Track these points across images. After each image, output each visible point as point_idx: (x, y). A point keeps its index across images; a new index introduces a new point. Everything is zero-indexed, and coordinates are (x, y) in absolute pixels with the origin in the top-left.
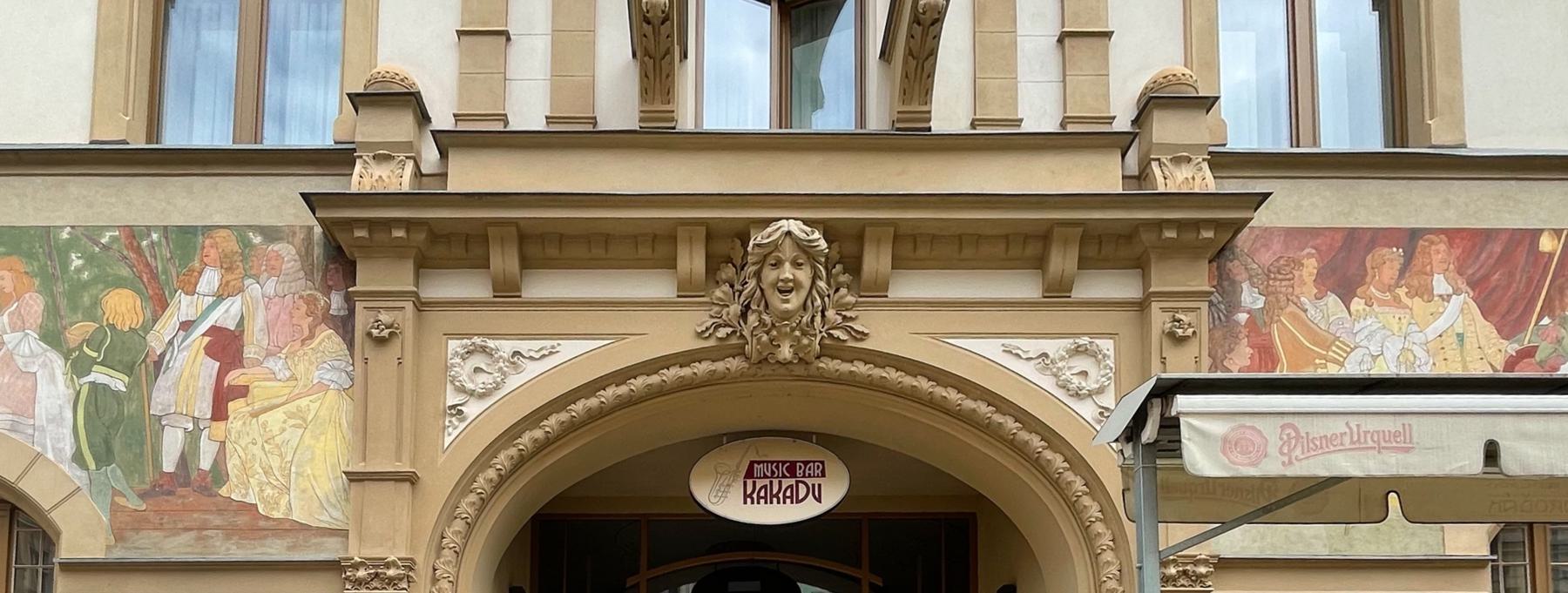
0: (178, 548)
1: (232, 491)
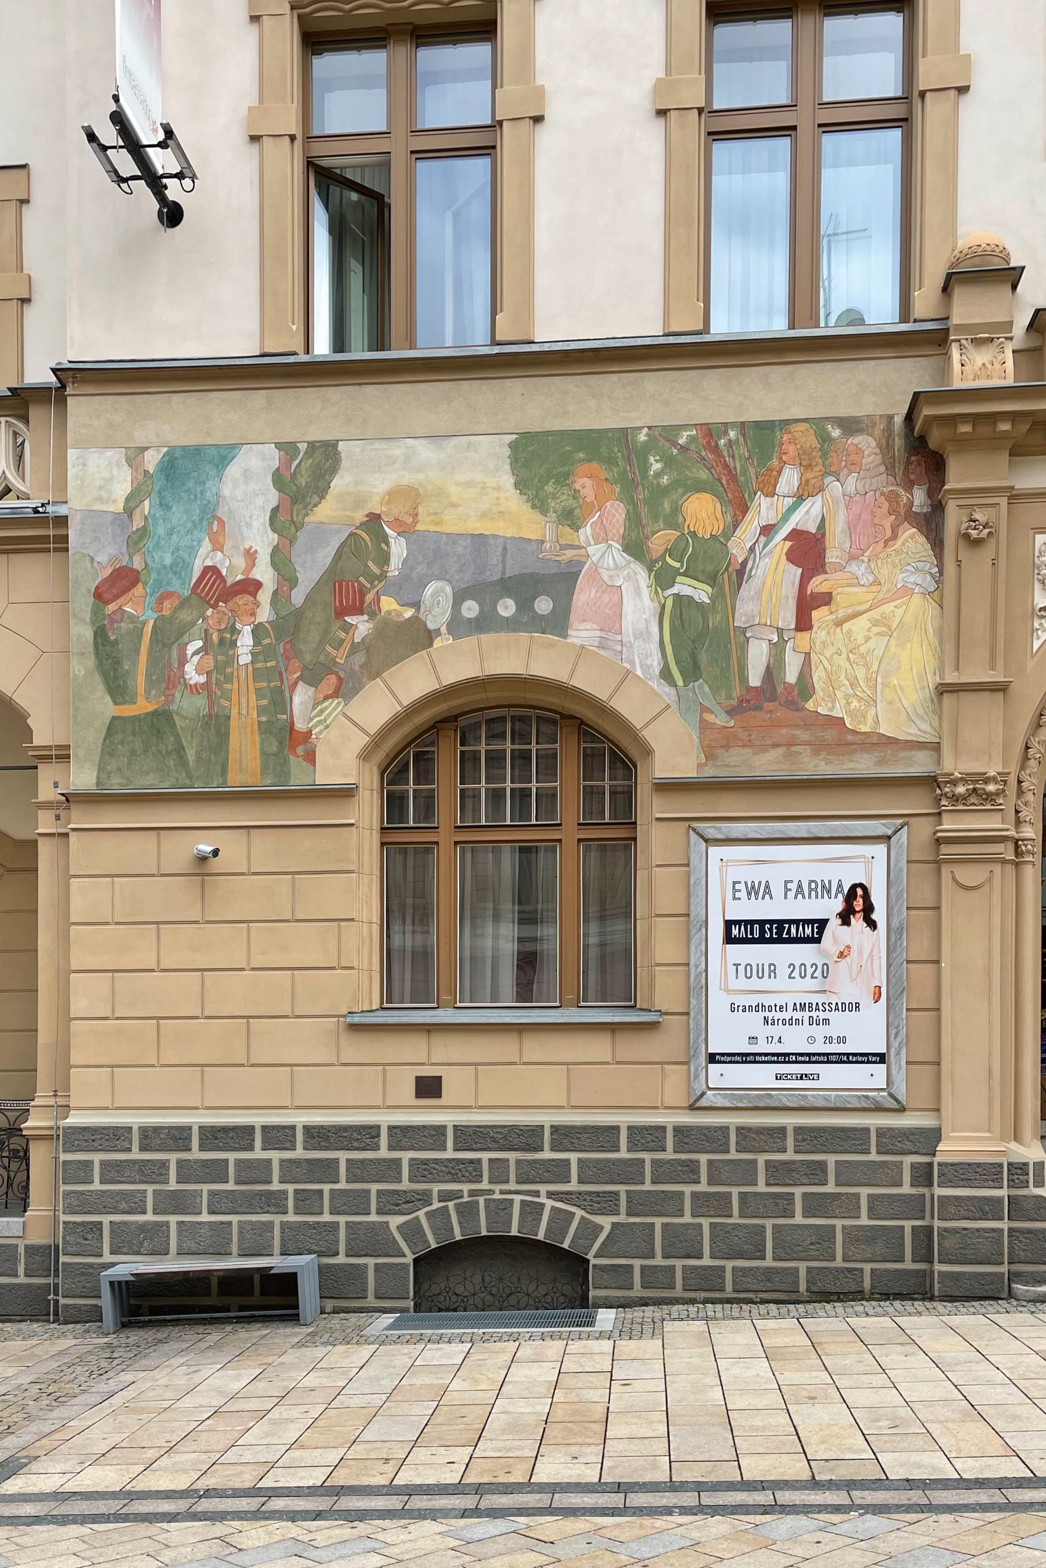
1: (819, 705)
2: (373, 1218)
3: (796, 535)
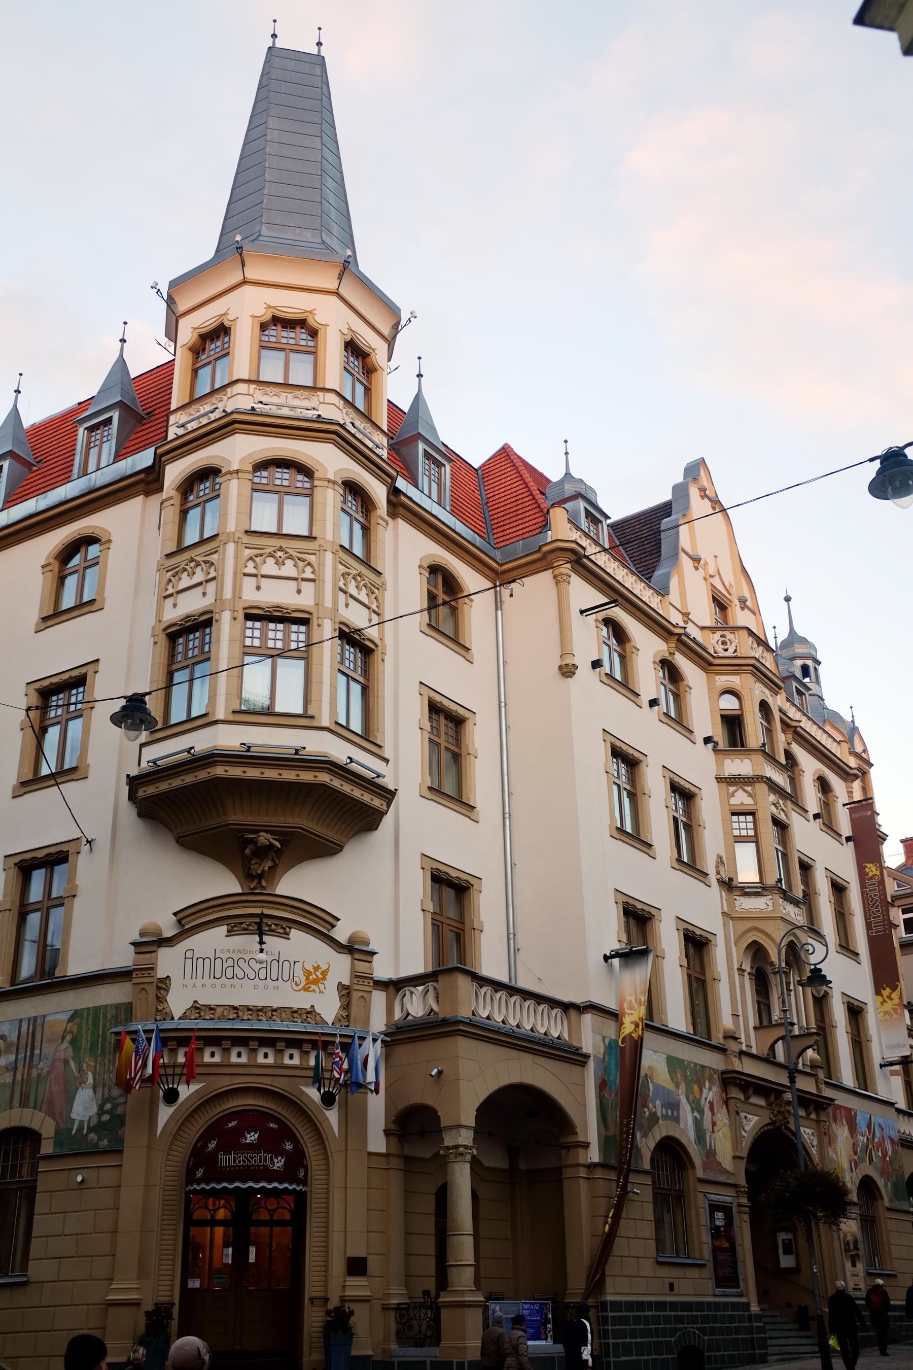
3: (710, 1102)
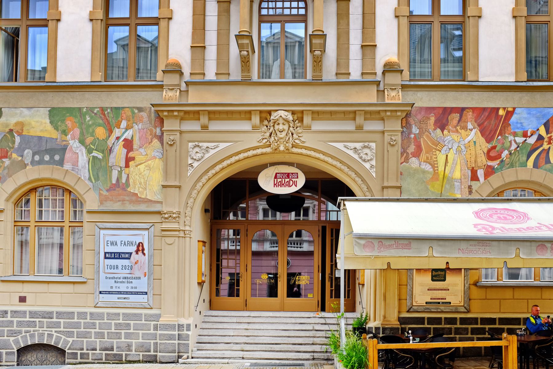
0: (117, 207)
1: (131, 189)
2: (6, 338)
3: (125, 140)
